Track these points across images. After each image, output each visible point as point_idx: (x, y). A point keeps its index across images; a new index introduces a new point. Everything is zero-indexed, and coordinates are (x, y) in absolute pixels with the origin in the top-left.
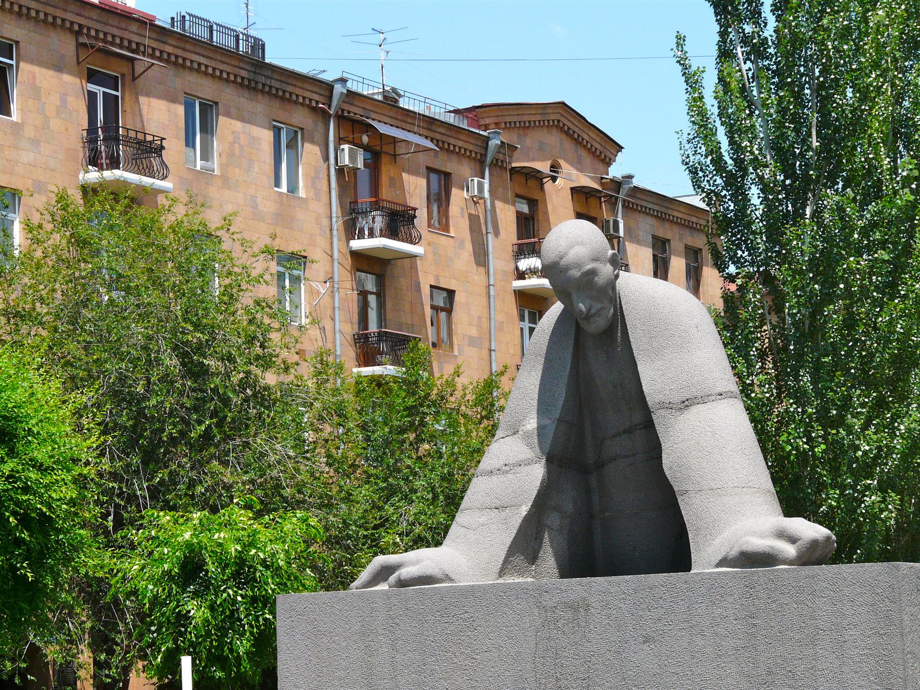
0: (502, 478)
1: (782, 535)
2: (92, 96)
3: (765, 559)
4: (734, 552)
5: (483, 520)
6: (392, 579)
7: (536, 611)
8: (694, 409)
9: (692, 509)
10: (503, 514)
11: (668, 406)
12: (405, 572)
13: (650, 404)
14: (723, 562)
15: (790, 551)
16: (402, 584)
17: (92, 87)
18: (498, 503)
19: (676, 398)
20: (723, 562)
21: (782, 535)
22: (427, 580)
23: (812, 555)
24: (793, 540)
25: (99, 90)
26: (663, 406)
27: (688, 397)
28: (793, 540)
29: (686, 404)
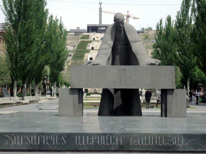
0: (105, 50)
1: (155, 61)
3: (154, 64)
4: (149, 63)
6: (92, 63)
9: (138, 57)
14: (148, 64)
15: (157, 64)
16: (94, 65)
19: (134, 40)
20: (148, 64)
22: (98, 64)
24: (157, 62)
26: (132, 42)
28: (157, 62)
29: (136, 42)
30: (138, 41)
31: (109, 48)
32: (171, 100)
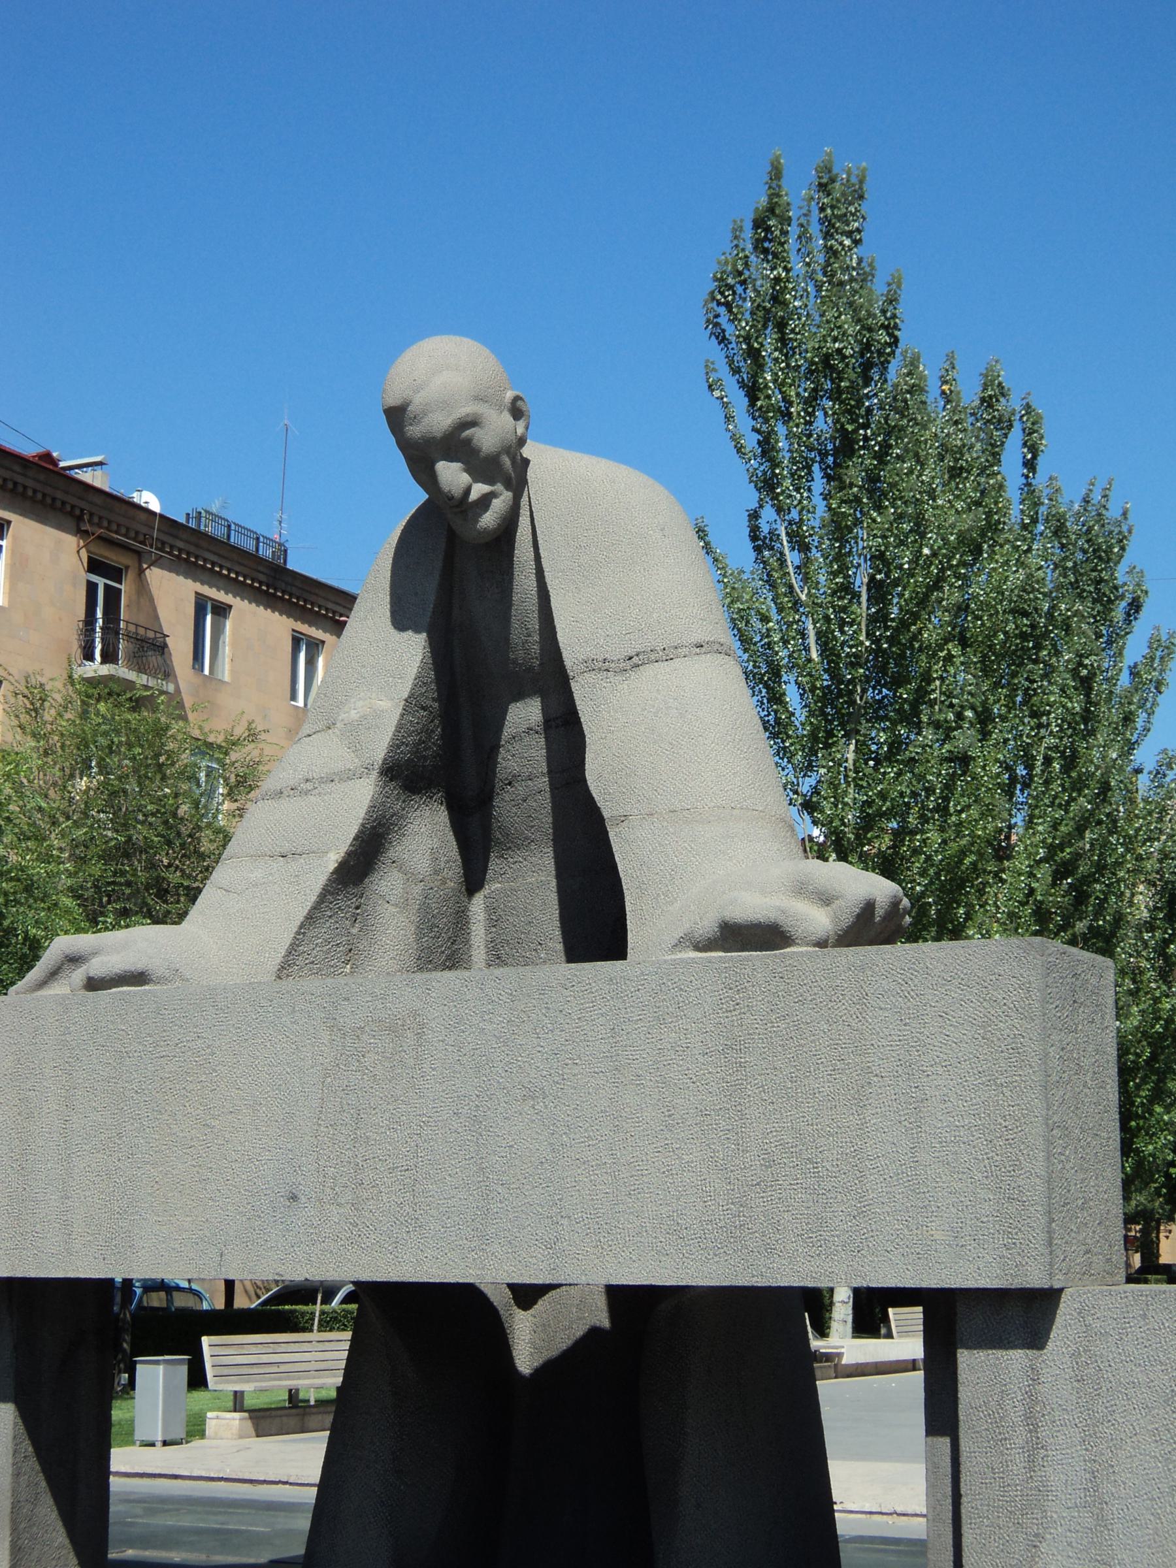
2: (91, 588)
5: (257, 875)
7: (325, 1036)
8: (649, 671)
10: (294, 866)
11: (603, 666)
12: (98, 967)
13: (568, 663)
15: (820, 920)
16: (93, 984)
17: (95, 578)
18: (286, 847)
19: (616, 651)
21: (801, 889)
22: (138, 978)
23: (867, 928)
24: (825, 899)
25: (101, 582)
27: (639, 648)
29: (634, 662)
30: (667, 655)
31: (349, 776)
32: (1018, 1462)
